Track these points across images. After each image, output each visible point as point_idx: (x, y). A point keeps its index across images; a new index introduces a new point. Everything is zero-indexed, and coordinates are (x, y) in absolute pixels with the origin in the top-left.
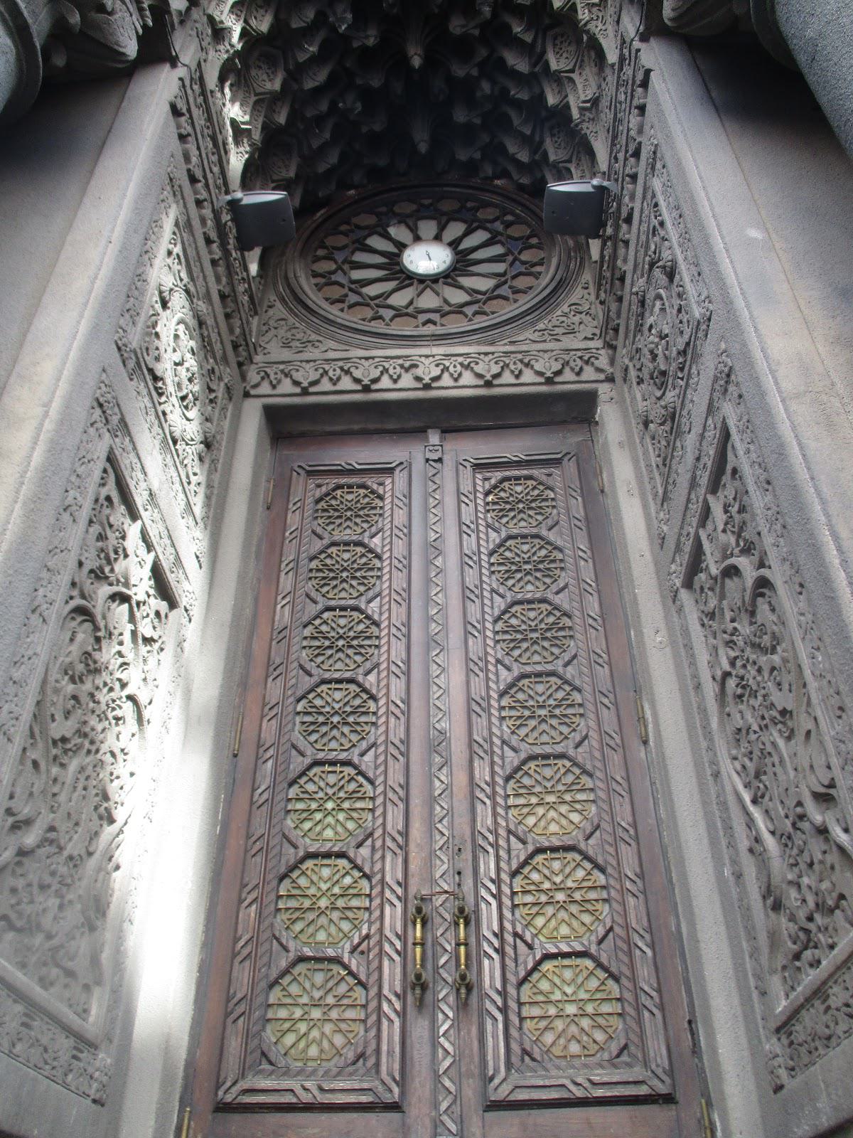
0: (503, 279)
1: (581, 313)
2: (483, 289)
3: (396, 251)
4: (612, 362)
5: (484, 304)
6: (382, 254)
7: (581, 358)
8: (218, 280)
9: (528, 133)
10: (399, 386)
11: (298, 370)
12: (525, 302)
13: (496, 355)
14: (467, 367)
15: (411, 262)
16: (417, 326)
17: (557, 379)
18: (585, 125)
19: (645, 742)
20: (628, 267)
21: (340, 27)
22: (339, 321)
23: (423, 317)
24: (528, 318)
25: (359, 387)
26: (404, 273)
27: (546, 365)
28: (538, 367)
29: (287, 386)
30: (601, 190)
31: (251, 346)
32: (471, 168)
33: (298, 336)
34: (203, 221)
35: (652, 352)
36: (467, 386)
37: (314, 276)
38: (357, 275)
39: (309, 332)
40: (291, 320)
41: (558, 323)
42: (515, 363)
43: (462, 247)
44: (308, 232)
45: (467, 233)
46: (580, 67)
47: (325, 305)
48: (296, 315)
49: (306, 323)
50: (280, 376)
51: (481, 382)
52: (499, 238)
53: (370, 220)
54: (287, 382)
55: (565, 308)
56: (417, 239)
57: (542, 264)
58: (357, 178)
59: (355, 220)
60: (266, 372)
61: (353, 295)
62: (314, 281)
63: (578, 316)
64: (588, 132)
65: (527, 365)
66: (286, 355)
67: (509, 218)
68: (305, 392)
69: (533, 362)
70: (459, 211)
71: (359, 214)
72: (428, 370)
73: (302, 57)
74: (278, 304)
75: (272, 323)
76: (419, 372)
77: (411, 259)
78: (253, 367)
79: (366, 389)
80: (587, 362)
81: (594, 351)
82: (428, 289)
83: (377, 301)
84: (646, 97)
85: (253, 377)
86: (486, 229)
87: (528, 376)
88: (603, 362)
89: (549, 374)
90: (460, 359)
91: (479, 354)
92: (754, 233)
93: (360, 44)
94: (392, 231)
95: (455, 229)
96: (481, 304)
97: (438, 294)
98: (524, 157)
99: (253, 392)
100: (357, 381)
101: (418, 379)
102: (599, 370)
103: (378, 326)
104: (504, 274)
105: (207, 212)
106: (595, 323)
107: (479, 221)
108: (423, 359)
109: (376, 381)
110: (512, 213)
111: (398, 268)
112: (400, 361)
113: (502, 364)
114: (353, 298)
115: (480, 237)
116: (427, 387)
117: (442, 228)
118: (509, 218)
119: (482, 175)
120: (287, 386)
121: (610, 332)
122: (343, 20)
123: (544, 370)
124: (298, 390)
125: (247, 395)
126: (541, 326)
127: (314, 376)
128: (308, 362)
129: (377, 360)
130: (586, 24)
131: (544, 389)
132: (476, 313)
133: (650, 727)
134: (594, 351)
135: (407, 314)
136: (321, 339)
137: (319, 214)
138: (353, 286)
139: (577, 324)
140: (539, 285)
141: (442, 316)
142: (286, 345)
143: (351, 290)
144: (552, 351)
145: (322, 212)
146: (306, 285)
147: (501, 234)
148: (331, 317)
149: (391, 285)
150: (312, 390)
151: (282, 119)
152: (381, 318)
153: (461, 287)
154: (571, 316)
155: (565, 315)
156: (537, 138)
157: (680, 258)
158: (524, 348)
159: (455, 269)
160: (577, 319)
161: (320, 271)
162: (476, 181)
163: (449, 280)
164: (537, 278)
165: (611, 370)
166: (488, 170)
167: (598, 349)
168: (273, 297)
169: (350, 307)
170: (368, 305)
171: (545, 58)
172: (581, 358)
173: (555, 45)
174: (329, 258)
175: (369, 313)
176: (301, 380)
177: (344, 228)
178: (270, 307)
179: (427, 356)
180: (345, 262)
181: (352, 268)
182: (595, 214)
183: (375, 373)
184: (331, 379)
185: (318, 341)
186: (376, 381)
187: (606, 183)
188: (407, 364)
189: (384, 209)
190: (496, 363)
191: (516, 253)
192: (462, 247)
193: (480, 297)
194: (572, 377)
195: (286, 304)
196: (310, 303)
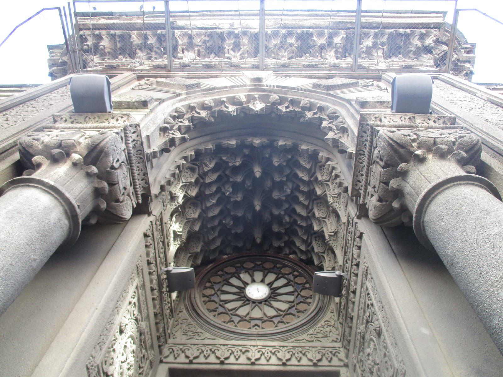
0: (293, 304)
1: (330, 326)
3: (243, 286)
4: (347, 356)
5: (283, 317)
6: (237, 287)
7: (331, 352)
8: (155, 307)
9: (305, 239)
10: (239, 362)
11: (189, 350)
12: (303, 318)
13: (288, 348)
14: (274, 354)
15: (250, 293)
16: (250, 328)
17: (320, 364)
18: (331, 242)
20: (355, 314)
21: (226, 193)
22: (212, 322)
23: (253, 323)
24: (305, 327)
25: (218, 362)
26: (246, 298)
27: (314, 355)
28: (309, 356)
29: (182, 359)
30: (340, 277)
31: (167, 335)
32: (280, 249)
33: (192, 329)
34: (151, 281)
35: (370, 369)
38: (224, 297)
39: (197, 327)
40: (190, 320)
41: (319, 331)
42: (298, 353)
43: (275, 285)
44: (203, 275)
45: (276, 279)
46: (329, 217)
47: (206, 312)
48: (192, 317)
49: (197, 322)
50: (180, 352)
51: (281, 363)
52: (291, 283)
53: (232, 270)
54: (183, 355)
55: (322, 323)
56: (253, 281)
57: (311, 298)
58: (228, 250)
59: (225, 270)
60: (172, 349)
61: (220, 309)
62: (203, 299)
63: (329, 328)
64: (333, 245)
65: (304, 354)
66: (184, 340)
67: (296, 273)
68: (191, 362)
69: (307, 353)
70: (273, 268)
71: (228, 266)
72: (254, 354)
73: (209, 205)
74: (184, 311)
75: (180, 321)
76: (249, 355)
77: (249, 291)
78: (167, 346)
79: (222, 363)
80: (334, 355)
81: (338, 349)
82: (257, 307)
83: (231, 312)
84: (361, 243)
85: (166, 351)
86: (285, 278)
87: (304, 361)
88: (342, 355)
89: (315, 361)
90: (271, 349)
91: (280, 346)
92: (425, 331)
93: (234, 200)
94: (242, 276)
95: (271, 277)
96: (281, 317)
97: (261, 310)
98: (303, 248)
99: (164, 360)
100: (218, 358)
101: (249, 359)
102: (340, 360)
103: (231, 327)
104: (293, 302)
105: (154, 277)
106: (337, 332)
107: (282, 274)
108: (252, 348)
109: (227, 358)
110: (298, 271)
111: (243, 295)
112: (240, 348)
113: (291, 353)
114: (221, 310)
115: (282, 282)
116: (253, 364)
117: (265, 276)
118: (296, 273)
119: (284, 253)
120: (182, 359)
121: (345, 340)
122: (228, 191)
123: (312, 358)
124: (187, 361)
125: (161, 362)
126: (311, 332)
127: (196, 353)
128: (194, 345)
129: (229, 346)
130: (331, 204)
131: (312, 369)
132: (279, 322)
134: (338, 349)
135: (246, 320)
136: (202, 331)
137: (209, 266)
138: (221, 303)
139: (329, 332)
140: (310, 309)
141: (263, 322)
142: (185, 334)
143: (220, 305)
144: (317, 347)
145: (211, 265)
146: (199, 301)
147: (292, 281)
148: (209, 320)
150: (195, 361)
151: (197, 228)
152: (233, 321)
153: (272, 307)
154: (325, 327)
155: (323, 327)
156: (309, 241)
157: (383, 325)
158: (303, 345)
159: (270, 297)
160: (328, 329)
161: (207, 294)
162: (281, 255)
163: (267, 303)
164: (309, 305)
165: (346, 361)
166: (287, 251)
167: (339, 348)
168: (183, 307)
169: (219, 314)
170: (227, 314)
171: (313, 211)
172: (331, 352)
173: (317, 206)
174: (211, 287)
175: (227, 318)
176: (189, 355)
177: (220, 273)
178: (180, 312)
179: (254, 346)
180: (219, 290)
181: (222, 294)
182: (336, 287)
183: (227, 354)
184: (205, 356)
185: (201, 333)
186: (227, 358)
187: (342, 274)
188: (244, 350)
189: (239, 265)
190: (288, 352)
191: (299, 291)
192: (275, 285)
193: (281, 313)
194: (327, 363)
195: (188, 311)
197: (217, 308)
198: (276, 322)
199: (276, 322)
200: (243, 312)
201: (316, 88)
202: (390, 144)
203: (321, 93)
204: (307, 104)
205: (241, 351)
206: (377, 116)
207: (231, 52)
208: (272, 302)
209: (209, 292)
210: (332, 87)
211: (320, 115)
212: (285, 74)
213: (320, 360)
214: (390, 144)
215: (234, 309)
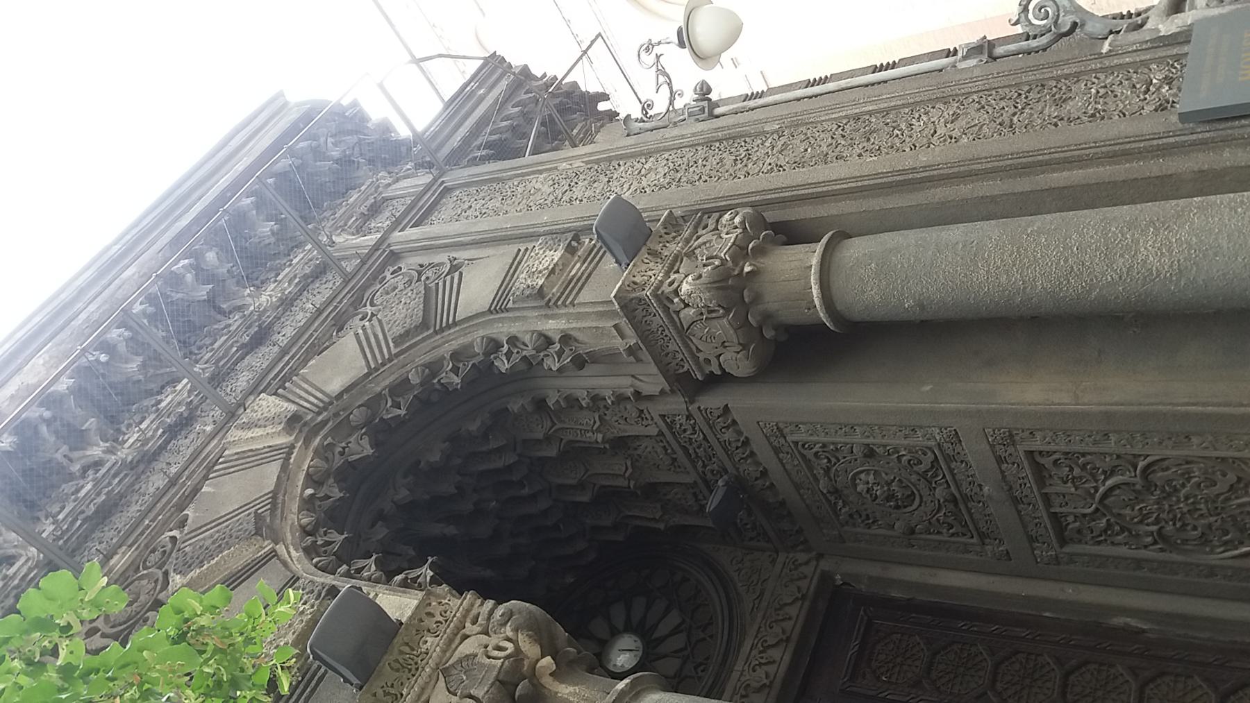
2: (677, 621)
16: (699, 678)
19: (1144, 631)
30: (727, 484)
36: (782, 657)
43: (620, 626)
88: (802, 557)
90: (754, 652)
97: (665, 656)
102: (807, 563)
131: (807, 604)
133: (1133, 622)
198: (702, 635)
201: (403, 343)
202: (718, 288)
203: (424, 340)
207: (76, 455)
208: (656, 635)
212: (274, 379)
213: (799, 589)
214: (718, 288)
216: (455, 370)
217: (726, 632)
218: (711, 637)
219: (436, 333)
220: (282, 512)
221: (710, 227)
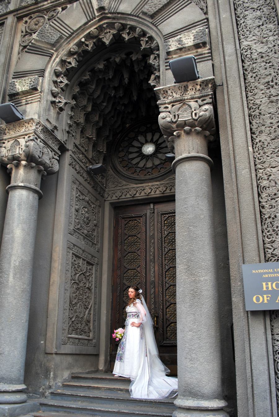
10: (141, 195)
36: (158, 194)
37: (119, 158)
39: (119, 179)
51: (161, 193)
62: (119, 160)
83: (135, 166)
90: (156, 186)
94: (139, 138)
103: (135, 176)
108: (146, 187)
112: (141, 188)
113: (166, 187)
120: (114, 198)
122: (112, 93)
137: (119, 136)
141: (152, 170)
146: (117, 162)
148: (124, 175)
149: (139, 159)
153: (158, 158)
168: (109, 167)
170: (133, 167)
174: (122, 151)
177: (126, 139)
178: (109, 171)
190: (165, 187)
196: (118, 170)
197: (128, 164)
199: (159, 169)
200: (141, 165)
203: (148, 21)
204: (140, 32)
205: (141, 189)
206: (164, 89)
209: (122, 154)
210: (155, 14)
211: (150, 44)
215: (137, 163)
216: (147, 42)
217: (160, 175)
218: (159, 171)
219: (151, 23)
220: (70, 41)
221: (201, 103)
